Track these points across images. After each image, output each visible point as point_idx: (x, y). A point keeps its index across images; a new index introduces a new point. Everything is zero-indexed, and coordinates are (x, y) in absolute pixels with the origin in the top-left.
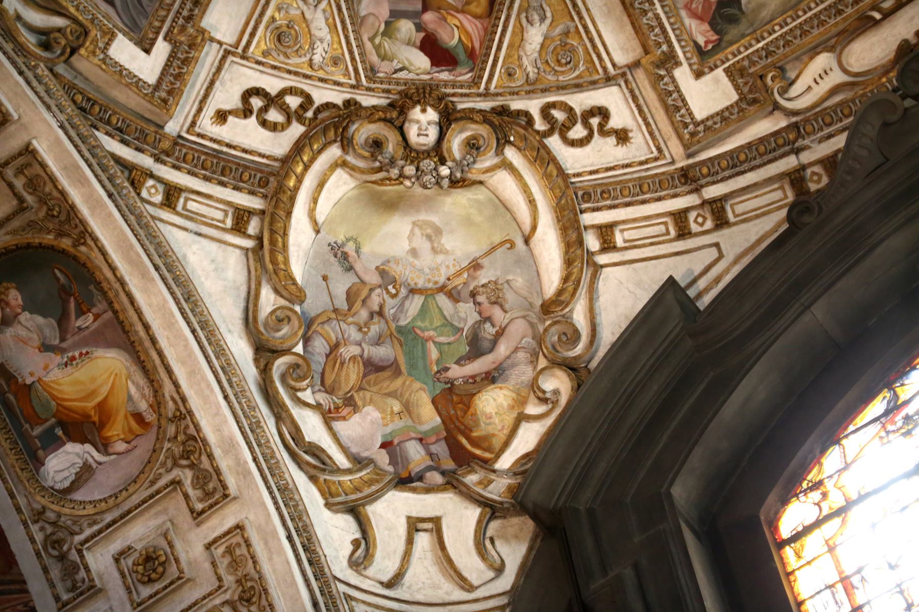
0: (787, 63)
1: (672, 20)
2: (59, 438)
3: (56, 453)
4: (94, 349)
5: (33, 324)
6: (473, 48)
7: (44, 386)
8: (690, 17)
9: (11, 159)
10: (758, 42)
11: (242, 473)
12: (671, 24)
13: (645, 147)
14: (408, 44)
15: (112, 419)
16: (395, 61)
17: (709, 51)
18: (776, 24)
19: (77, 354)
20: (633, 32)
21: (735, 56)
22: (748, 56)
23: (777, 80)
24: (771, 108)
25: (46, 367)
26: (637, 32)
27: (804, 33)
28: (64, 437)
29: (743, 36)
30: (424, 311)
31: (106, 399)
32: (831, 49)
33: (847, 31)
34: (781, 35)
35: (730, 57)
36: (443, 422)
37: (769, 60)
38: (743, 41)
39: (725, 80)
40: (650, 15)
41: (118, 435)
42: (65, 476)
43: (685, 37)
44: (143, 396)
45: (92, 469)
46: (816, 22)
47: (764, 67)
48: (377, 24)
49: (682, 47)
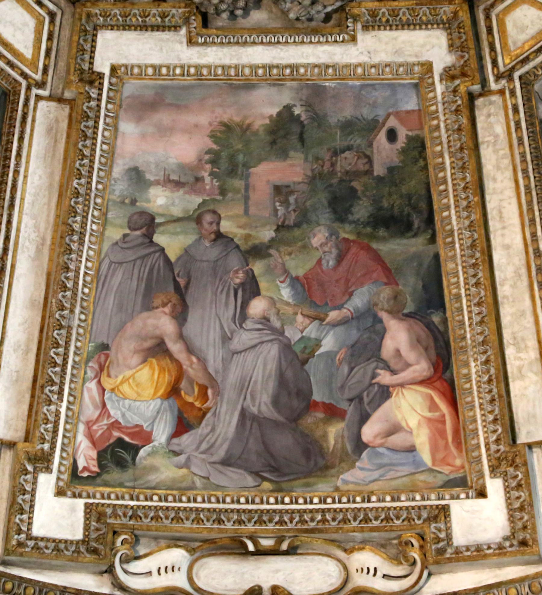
0: (144, 536)
1: (68, 427)
8: (85, 435)
10: (132, 499)
12: (65, 430)
17: (82, 477)
18: (157, 494)
20: (26, 413)
21: (103, 497)
22: (115, 505)
23: (127, 546)
24: (104, 568)
26: (29, 416)
27: (177, 519)
29: (121, 485)
32: (191, 551)
33: (215, 543)
34: (156, 507)
35: (98, 495)
37: (131, 522)
38: (118, 489)
39: (81, 514)
40: (53, 408)
43: (70, 450)
46: (193, 516)
47: (124, 526)
49: (62, 457)
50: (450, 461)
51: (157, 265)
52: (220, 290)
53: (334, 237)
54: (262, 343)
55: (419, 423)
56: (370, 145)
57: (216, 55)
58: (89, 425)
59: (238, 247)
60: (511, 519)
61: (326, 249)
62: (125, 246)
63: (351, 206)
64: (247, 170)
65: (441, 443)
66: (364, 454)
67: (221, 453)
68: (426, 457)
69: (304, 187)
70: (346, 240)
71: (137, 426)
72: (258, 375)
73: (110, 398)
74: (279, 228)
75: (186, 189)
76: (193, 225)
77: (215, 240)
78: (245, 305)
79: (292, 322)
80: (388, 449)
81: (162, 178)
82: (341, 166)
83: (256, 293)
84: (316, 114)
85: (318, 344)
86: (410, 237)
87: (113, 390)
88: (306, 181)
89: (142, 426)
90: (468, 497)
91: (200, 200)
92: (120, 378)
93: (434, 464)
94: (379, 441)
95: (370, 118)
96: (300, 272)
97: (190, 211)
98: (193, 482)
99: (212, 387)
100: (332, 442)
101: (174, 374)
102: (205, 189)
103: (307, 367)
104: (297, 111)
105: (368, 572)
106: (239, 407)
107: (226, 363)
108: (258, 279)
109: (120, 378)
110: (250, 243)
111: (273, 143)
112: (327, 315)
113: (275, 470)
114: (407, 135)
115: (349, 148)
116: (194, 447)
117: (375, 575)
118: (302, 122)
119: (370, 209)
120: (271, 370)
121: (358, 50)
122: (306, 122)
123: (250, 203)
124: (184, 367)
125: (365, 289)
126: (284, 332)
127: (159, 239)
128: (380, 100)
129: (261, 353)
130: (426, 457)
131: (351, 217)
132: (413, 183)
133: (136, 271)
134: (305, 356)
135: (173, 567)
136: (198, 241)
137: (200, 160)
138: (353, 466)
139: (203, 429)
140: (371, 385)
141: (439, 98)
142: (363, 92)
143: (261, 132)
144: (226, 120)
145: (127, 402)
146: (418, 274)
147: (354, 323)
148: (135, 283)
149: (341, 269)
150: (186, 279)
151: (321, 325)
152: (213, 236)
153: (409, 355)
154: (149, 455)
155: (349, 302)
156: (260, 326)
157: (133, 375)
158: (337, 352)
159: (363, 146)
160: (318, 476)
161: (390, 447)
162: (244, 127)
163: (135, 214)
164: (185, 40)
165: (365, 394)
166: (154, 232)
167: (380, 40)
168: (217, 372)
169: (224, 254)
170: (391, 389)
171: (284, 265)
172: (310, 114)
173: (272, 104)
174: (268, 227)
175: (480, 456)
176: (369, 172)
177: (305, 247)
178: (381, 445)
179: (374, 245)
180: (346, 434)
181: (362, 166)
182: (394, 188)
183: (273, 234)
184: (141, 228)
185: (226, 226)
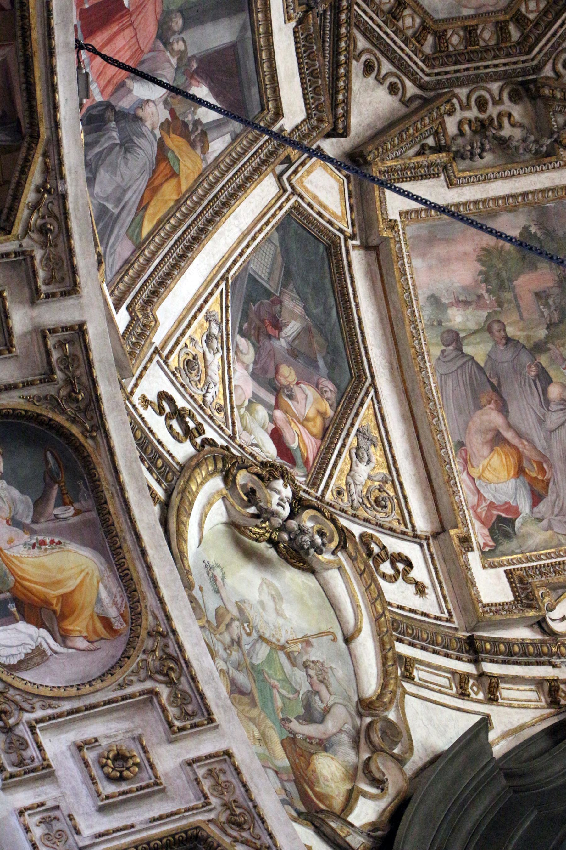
2: (12, 614)
3: (5, 627)
4: (68, 542)
5: (7, 495)
6: (307, 458)
7: (5, 558)
9: (62, 328)
11: (223, 707)
13: (437, 606)
14: (263, 427)
15: (75, 615)
16: (252, 437)
19: (48, 540)
25: (10, 541)
28: (17, 615)
30: (269, 659)
31: (72, 592)
36: (291, 765)
41: (80, 632)
42: (13, 653)
44: (115, 603)
45: (46, 655)
48: (243, 398)
51: (473, 373)
52: (523, 383)
58: (474, 508)
59: (524, 346)
62: (446, 360)
69: (557, 290)
71: (506, 503)
73: (480, 484)
74: (548, 328)
75: (474, 306)
76: (487, 335)
77: (506, 344)
78: (545, 391)
81: (454, 301)
84: (547, 230)
87: (479, 478)
91: (486, 314)
92: (481, 467)
98: (559, 540)
99: (546, 462)
102: (487, 304)
104: (533, 230)
108: (547, 369)
109: (481, 467)
118: (539, 238)
122: (541, 238)
124: (521, 450)
127: (467, 350)
133: (460, 379)
136: (495, 346)
137: (476, 281)
139: (551, 497)
144: (484, 246)
148: (463, 389)
152: (504, 341)
156: (562, 407)
157: (489, 462)
163: (444, 332)
164: (445, 184)
166: (462, 345)
168: (545, 450)
169: (515, 355)
171: (561, 355)
172: (542, 230)
174: (541, 327)
183: (546, 332)
184: (452, 343)
185: (511, 331)
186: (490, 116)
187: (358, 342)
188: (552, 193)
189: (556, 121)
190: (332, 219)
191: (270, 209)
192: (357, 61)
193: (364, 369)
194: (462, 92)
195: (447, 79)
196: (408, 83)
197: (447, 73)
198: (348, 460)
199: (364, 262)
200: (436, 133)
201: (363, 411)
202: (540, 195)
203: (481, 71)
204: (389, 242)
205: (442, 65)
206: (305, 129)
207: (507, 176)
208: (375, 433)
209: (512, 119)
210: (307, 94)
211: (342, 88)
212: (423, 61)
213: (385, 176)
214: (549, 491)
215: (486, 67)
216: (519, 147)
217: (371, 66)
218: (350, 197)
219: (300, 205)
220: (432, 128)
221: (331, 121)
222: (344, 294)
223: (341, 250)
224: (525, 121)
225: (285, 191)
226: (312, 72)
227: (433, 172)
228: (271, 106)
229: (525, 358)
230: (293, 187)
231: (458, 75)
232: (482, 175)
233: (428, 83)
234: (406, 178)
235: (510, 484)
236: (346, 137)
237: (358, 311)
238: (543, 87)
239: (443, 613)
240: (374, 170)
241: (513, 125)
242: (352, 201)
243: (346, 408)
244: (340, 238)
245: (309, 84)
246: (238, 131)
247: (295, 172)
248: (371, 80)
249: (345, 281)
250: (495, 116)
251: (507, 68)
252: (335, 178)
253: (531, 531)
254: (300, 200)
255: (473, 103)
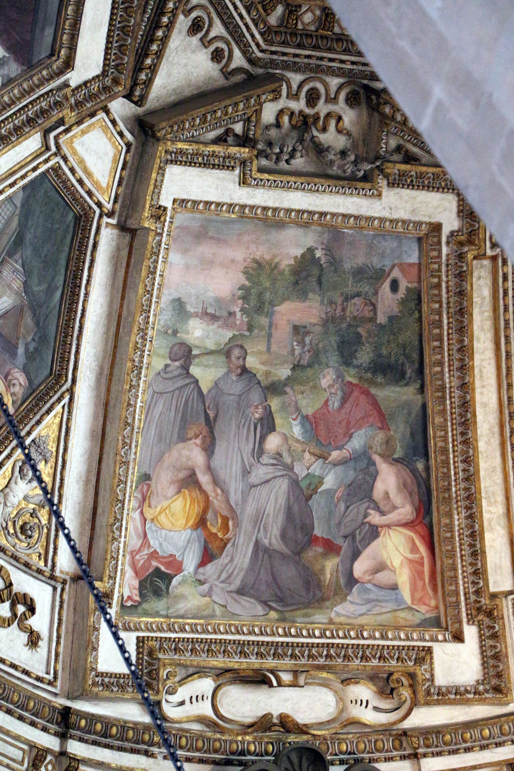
13: (45, 663)
33: (238, 673)
50: (427, 601)
52: (242, 424)
53: (340, 379)
54: (275, 477)
55: (401, 563)
56: (376, 293)
57: (263, 197)
58: (133, 554)
59: (259, 383)
60: (484, 664)
61: (333, 391)
62: (165, 376)
63: (356, 351)
64: (272, 308)
65: (420, 584)
66: (355, 589)
67: (237, 583)
68: (406, 594)
69: (318, 329)
70: (350, 383)
71: (171, 555)
72: (270, 509)
73: (150, 528)
75: (220, 323)
76: (223, 359)
77: (241, 375)
78: (263, 439)
79: (301, 459)
80: (375, 585)
81: (200, 311)
82: (351, 312)
83: (272, 428)
84: (333, 258)
85: (321, 482)
86: (403, 386)
87: (152, 520)
88: (320, 323)
89: (175, 556)
90: (445, 640)
91: (230, 334)
92: (159, 508)
93: (413, 603)
94: (367, 578)
95: (378, 267)
96: (309, 411)
97: (220, 344)
98: (214, 611)
99: (233, 519)
100: (328, 576)
101: (202, 505)
102: (236, 324)
103: (310, 503)
104: (318, 254)
105: (361, 705)
106: (254, 540)
107: (245, 495)
108: (274, 415)
109: (159, 508)
110: (270, 380)
111: (296, 283)
112: (330, 454)
113: (280, 600)
114: (407, 287)
115: (358, 295)
116: (215, 577)
117: (366, 707)
118: (321, 265)
119: (371, 355)
120: (281, 505)
121: (381, 204)
122: (324, 266)
123: (272, 341)
124: (211, 498)
125: (362, 432)
126: (293, 469)
127: (194, 370)
128: (388, 251)
129: (274, 487)
130: (406, 594)
131: (355, 362)
132: (409, 332)
133: (174, 401)
134: (310, 492)
135: (203, 696)
136: (227, 374)
137: (234, 295)
138: (344, 600)
139: (224, 559)
140: (363, 524)
141: (444, 258)
142: (375, 242)
143: (286, 272)
144: (258, 258)
145: (163, 531)
146: (407, 422)
147: (352, 464)
148: (173, 414)
149: (344, 411)
150: (215, 412)
151: (324, 463)
152: (239, 371)
153: (397, 498)
154: (179, 584)
155: (349, 444)
156: (274, 462)
157: (169, 506)
158: (336, 491)
159: (370, 293)
160: (315, 607)
161: (376, 583)
162: (273, 265)
164: (237, 180)
165: (358, 531)
166: (191, 363)
167: (401, 197)
168: (237, 505)
169: (247, 389)
170: (380, 529)
171: (296, 402)
172: (328, 257)
173: (298, 245)
175: (458, 603)
176: (373, 320)
177: (314, 387)
178: (369, 581)
179: (373, 391)
180: (340, 568)
181: (368, 314)
182: (392, 337)
184: (180, 359)
185: (251, 362)
186: (317, 113)
187: (72, 336)
188: (355, 219)
189: (386, 144)
190: (93, 190)
191: (22, 167)
192: (186, 16)
193: (67, 369)
194: (296, 78)
195: (283, 61)
196: (237, 53)
197: (284, 54)
198: (8, 474)
199: (114, 244)
200: (248, 120)
201: (48, 419)
202: (340, 218)
203: (323, 63)
204: (148, 234)
205: (283, 43)
206: (94, 87)
207: (310, 190)
208: (52, 447)
209: (341, 124)
210: (111, 48)
211: (154, 52)
212: (262, 34)
213: (171, 156)
214: (225, 553)
215: (331, 60)
216: (334, 161)
217: (199, 25)
218: (123, 169)
219: (60, 167)
220: (244, 114)
221: (128, 86)
222: (77, 276)
223: (91, 226)
224: (354, 131)
225: (48, 149)
226: (123, 27)
227: (228, 164)
228: (63, 52)
229: (255, 396)
230: (58, 146)
231: (297, 60)
232: (282, 182)
233: (259, 59)
234: (195, 163)
235: (184, 535)
236: (140, 106)
237: (85, 301)
238: (385, 104)
239: (48, 673)
240: (160, 148)
241: (339, 131)
242: (124, 173)
243: (31, 410)
244: (95, 212)
245: (116, 38)
246: (13, 75)
247: (67, 131)
248: (195, 40)
249: (84, 262)
250: (322, 115)
251: (355, 67)
252: (113, 144)
253: (187, 594)
254: (62, 163)
255: (303, 94)
